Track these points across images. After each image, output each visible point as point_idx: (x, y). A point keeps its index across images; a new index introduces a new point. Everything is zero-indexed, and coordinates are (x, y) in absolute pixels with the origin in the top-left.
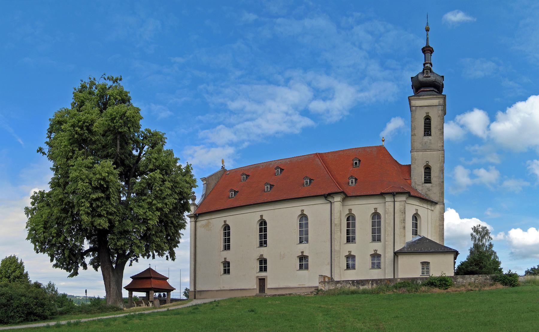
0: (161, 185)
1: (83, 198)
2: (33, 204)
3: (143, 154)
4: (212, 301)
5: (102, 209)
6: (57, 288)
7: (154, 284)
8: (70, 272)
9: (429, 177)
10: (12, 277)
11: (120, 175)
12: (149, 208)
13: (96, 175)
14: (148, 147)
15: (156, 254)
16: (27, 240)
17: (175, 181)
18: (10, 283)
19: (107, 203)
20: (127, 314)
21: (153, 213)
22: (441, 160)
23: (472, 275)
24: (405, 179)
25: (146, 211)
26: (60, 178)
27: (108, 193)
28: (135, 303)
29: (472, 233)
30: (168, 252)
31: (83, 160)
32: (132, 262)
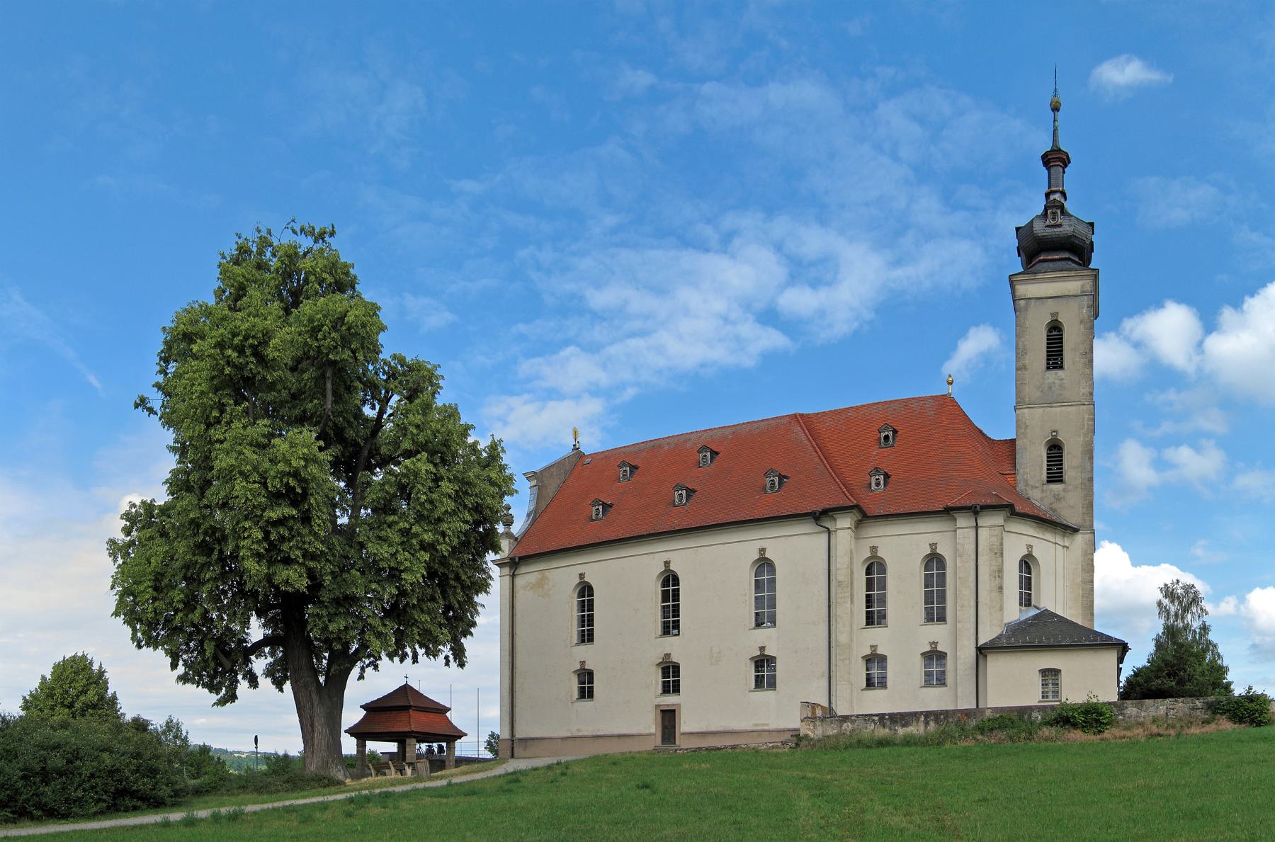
0: (430, 488)
1: (246, 518)
2: (127, 531)
3: (388, 414)
4: (553, 764)
5: (291, 544)
6: (187, 733)
7: (417, 722)
8: (217, 695)
9: (1058, 469)
10: (78, 705)
11: (335, 464)
12: (402, 543)
13: (276, 464)
14: (399, 398)
15: (421, 652)
16: (114, 617)
17: (463, 479)
18: (72, 720)
19: (305, 531)
20: (353, 794)
21: (413, 555)
22: (1086, 426)
23: (1159, 700)
24: (1002, 474)
25: (397, 551)
26: (192, 470)
27: (306, 507)
28: (371, 767)
29: (1160, 601)
30: (449, 647)
31: (245, 427)
32: (364, 671)
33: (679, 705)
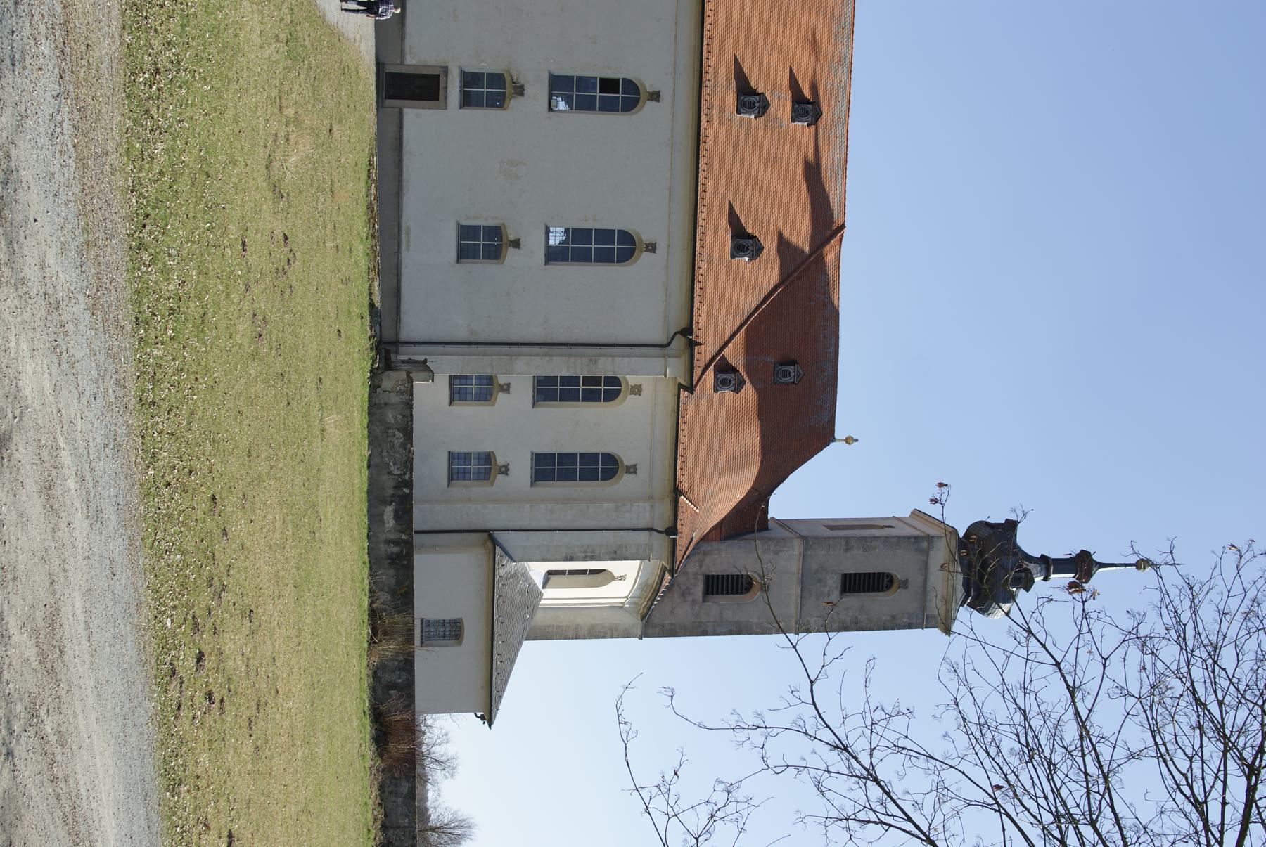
33: (446, 108)
